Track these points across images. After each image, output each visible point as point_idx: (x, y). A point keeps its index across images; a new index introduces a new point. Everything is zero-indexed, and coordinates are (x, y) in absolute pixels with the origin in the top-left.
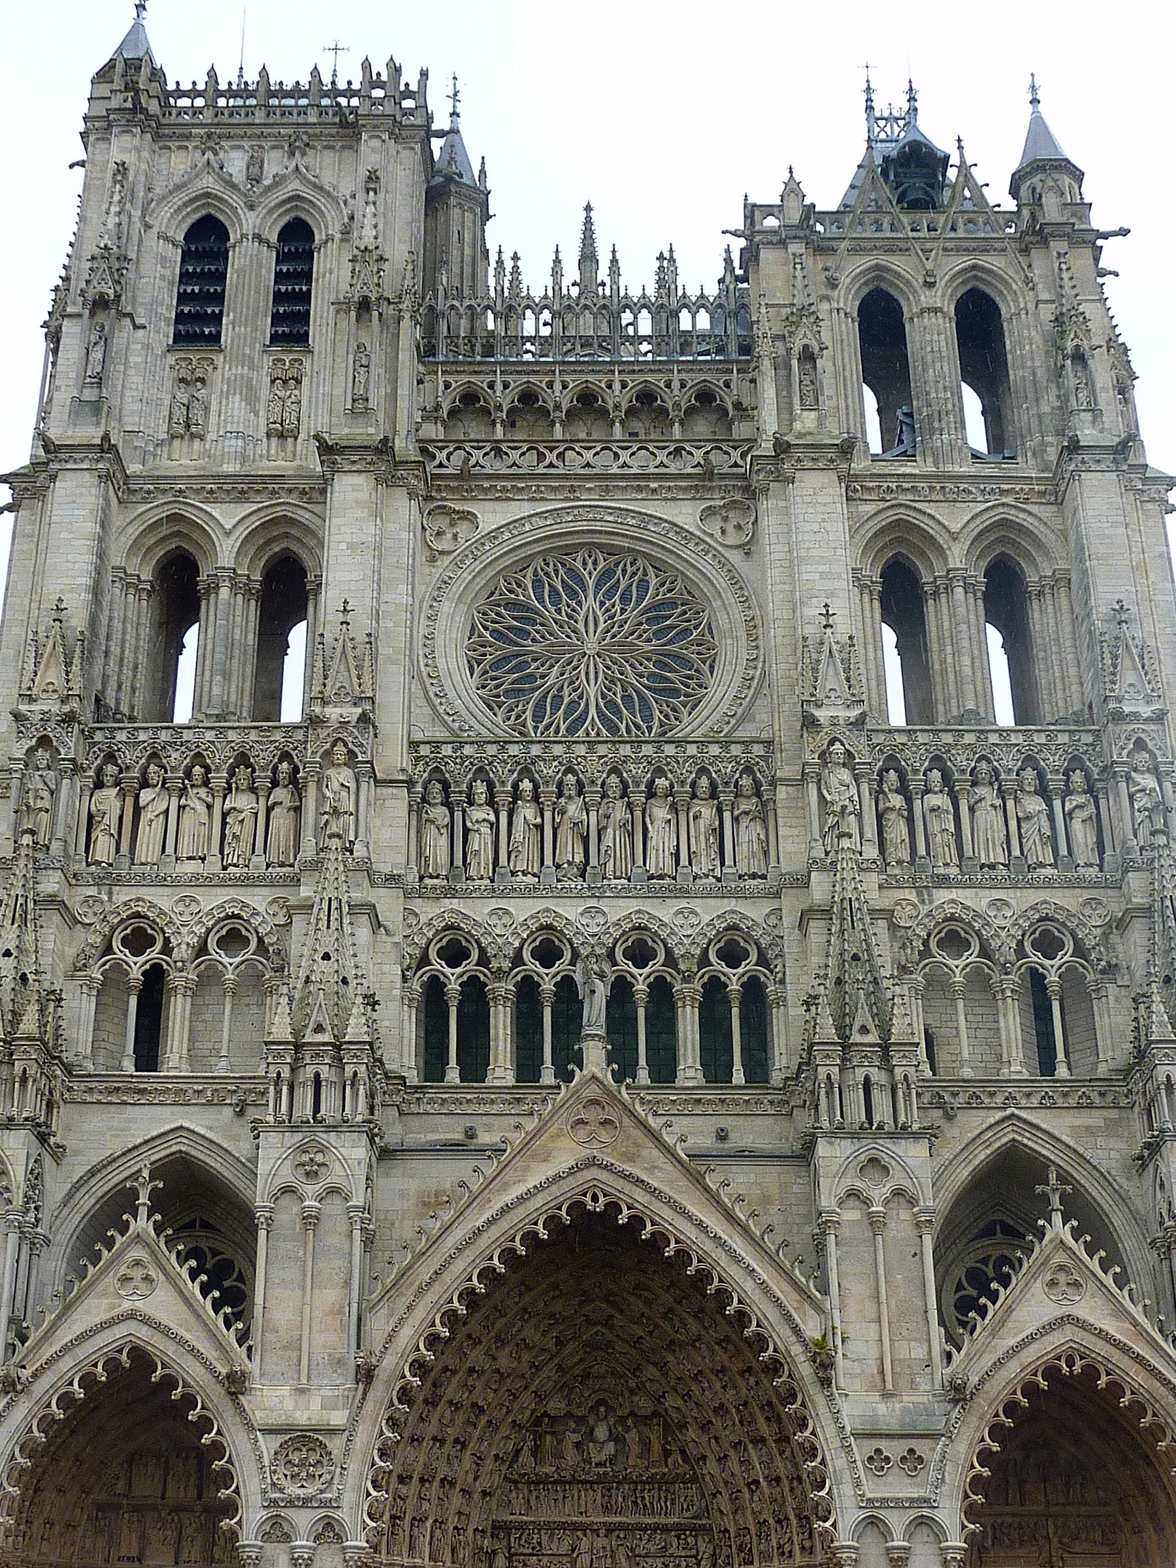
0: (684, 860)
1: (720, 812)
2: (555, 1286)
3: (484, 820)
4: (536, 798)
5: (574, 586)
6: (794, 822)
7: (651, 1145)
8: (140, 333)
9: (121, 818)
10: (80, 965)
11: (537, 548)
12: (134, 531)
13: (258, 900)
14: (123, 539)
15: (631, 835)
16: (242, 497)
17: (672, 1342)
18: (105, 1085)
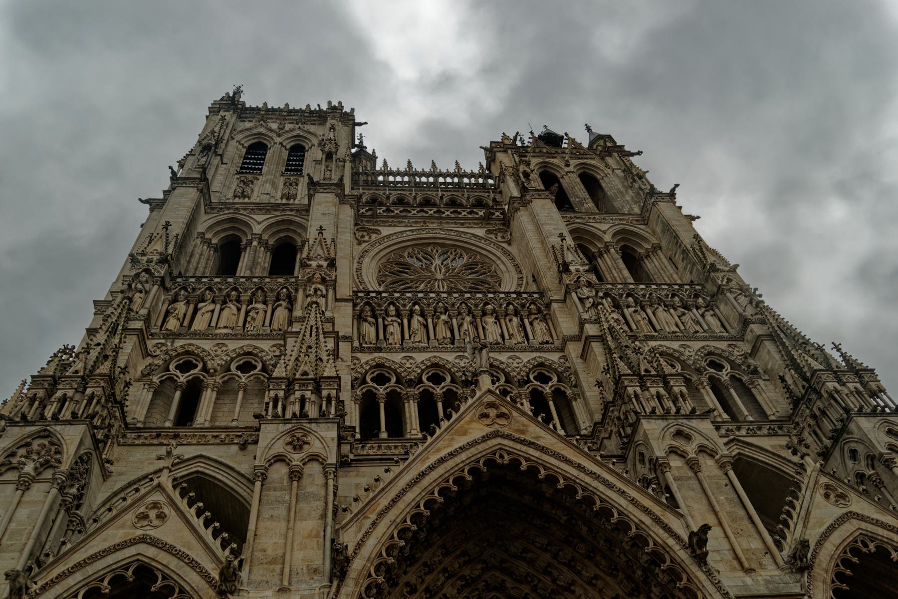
0: (507, 336)
1: (522, 320)
2: (464, 553)
3: (395, 321)
4: (422, 314)
5: (429, 257)
6: (565, 316)
7: (534, 425)
8: (225, 166)
9: (185, 315)
10: (145, 373)
11: (409, 243)
12: (210, 222)
13: (265, 345)
14: (205, 224)
15: (477, 328)
16: (268, 211)
17: (553, 591)
18: (149, 434)
